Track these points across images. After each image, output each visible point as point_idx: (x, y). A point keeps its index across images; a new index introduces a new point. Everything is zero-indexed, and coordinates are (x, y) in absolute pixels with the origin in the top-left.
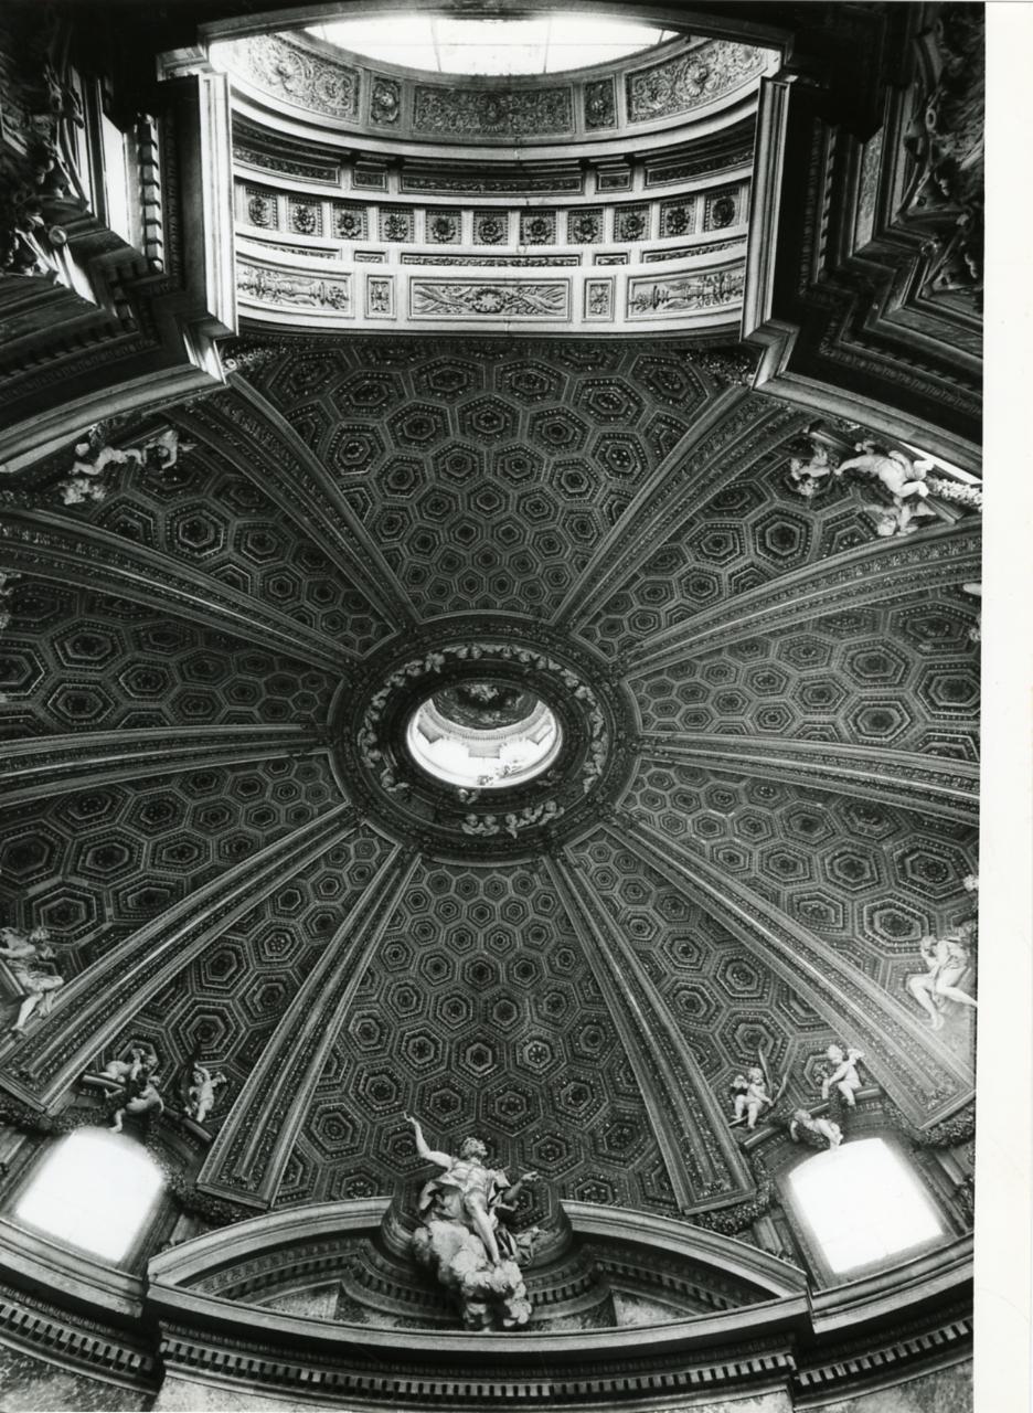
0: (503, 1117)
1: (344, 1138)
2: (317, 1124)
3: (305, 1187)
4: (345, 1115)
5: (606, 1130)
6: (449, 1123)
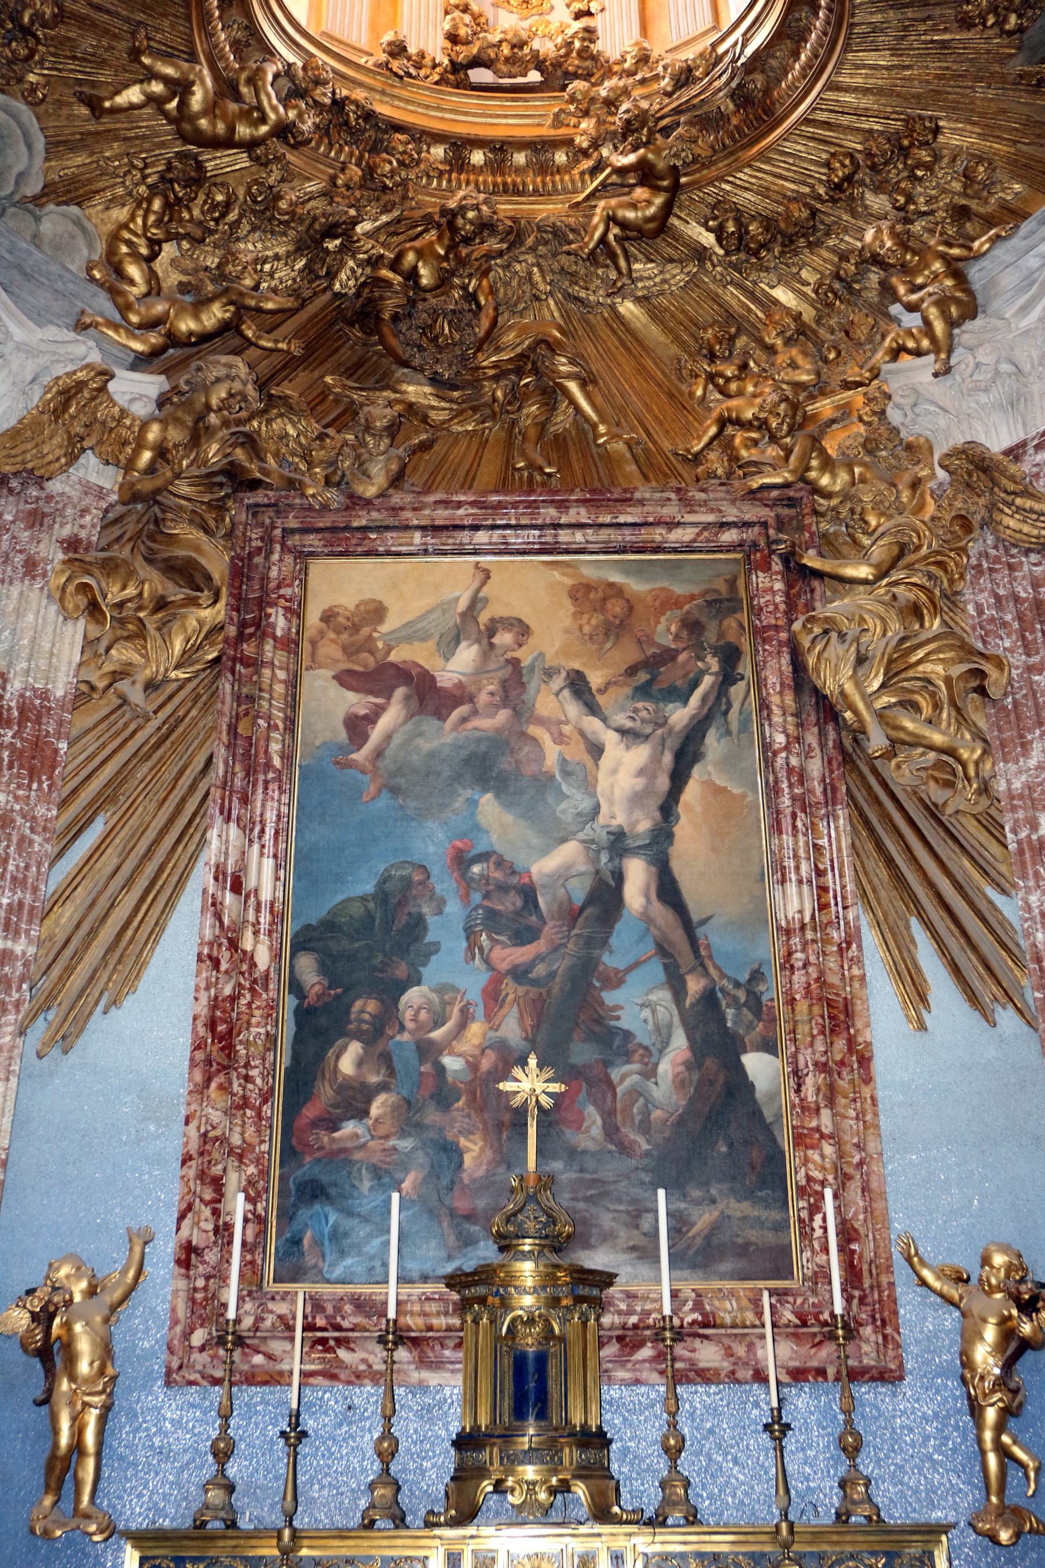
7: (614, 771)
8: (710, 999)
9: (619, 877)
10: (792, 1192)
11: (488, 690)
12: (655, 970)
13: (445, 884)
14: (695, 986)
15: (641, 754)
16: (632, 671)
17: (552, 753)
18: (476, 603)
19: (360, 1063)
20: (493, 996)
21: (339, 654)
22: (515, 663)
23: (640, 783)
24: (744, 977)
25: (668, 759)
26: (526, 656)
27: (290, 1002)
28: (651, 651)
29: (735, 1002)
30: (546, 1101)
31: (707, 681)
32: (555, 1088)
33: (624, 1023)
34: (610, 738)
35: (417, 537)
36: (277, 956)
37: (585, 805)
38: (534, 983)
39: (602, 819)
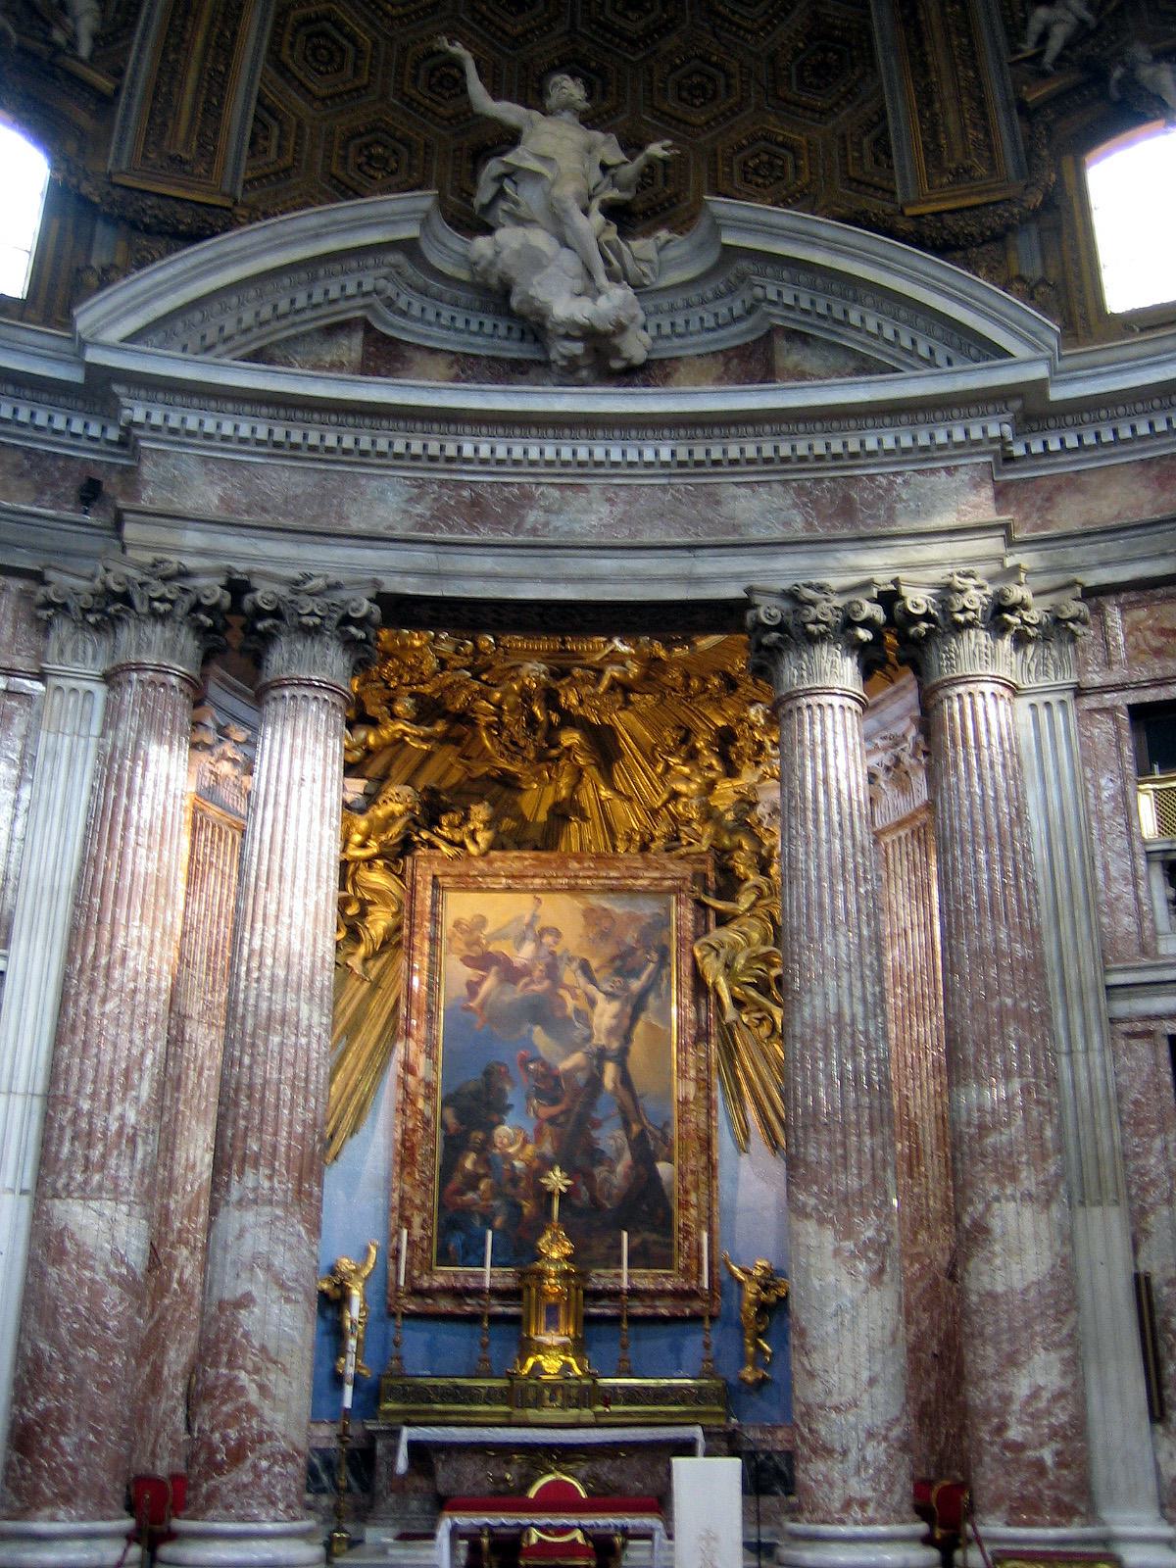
0: (621, 22)
1: (341, 68)
2: (292, 46)
3: (287, 160)
4: (339, 25)
5: (797, 52)
6: (524, 35)
7: (601, 1016)
8: (642, 1134)
9: (602, 1071)
10: (676, 1230)
11: (539, 969)
12: (618, 1120)
13: (516, 1072)
14: (635, 1128)
15: (614, 1007)
16: (613, 959)
17: (571, 1003)
18: (535, 917)
19: (475, 1164)
20: (539, 1132)
21: (462, 946)
22: (552, 953)
23: (614, 1022)
24: (660, 1124)
25: (629, 1009)
26: (558, 950)
27: (440, 1133)
28: (623, 948)
29: (655, 1138)
30: (563, 1189)
31: (651, 966)
32: (569, 1182)
33: (601, 1147)
34: (600, 997)
35: (504, 880)
36: (435, 1110)
37: (586, 1032)
38: (558, 1125)
39: (594, 1041)
